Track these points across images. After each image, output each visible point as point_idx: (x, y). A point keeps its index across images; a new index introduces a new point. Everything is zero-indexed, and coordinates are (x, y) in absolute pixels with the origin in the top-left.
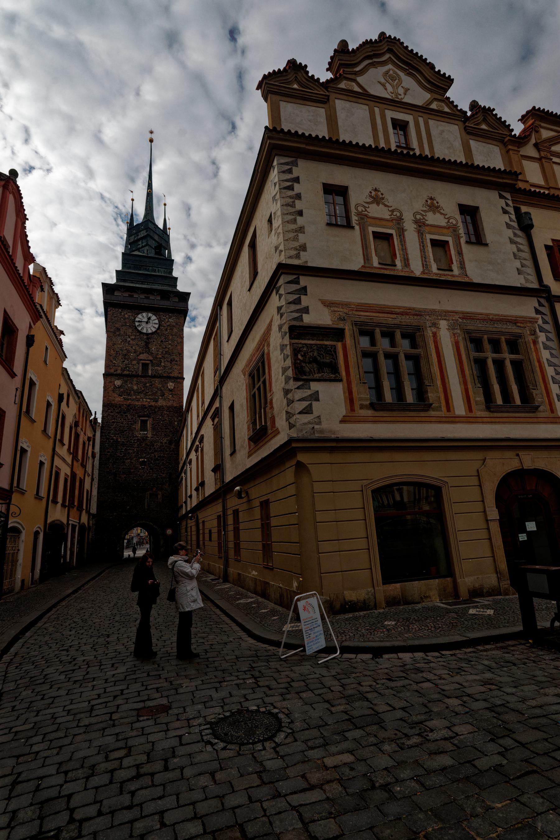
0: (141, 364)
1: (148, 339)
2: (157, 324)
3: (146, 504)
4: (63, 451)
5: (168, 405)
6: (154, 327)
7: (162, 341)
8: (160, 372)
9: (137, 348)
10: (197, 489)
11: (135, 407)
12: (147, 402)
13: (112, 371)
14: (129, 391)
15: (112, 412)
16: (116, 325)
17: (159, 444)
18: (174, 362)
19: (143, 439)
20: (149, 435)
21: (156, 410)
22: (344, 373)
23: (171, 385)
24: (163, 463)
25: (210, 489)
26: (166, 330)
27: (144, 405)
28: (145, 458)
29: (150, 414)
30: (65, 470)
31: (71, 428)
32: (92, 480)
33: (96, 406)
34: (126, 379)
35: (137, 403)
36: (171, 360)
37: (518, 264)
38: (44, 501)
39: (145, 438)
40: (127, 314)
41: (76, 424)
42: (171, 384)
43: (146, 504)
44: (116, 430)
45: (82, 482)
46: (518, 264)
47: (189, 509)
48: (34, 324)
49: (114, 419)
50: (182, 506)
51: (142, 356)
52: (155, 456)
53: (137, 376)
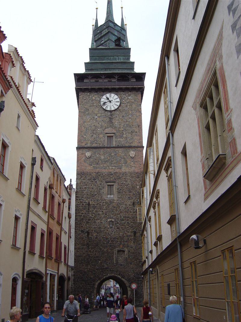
0: (106, 137)
1: (111, 115)
2: (118, 102)
3: (115, 259)
4: (39, 209)
5: (130, 171)
6: (116, 105)
7: (123, 116)
8: (123, 142)
9: (103, 124)
10: (156, 244)
11: (102, 174)
12: (112, 169)
13: (83, 145)
14: (97, 161)
15: (84, 180)
16: (86, 107)
17: (124, 206)
18: (134, 133)
19: (111, 202)
20: (116, 199)
21: (120, 176)
23: (132, 153)
24: (128, 223)
25: (166, 242)
26: (127, 106)
27: (110, 172)
28: (112, 218)
29: (115, 179)
30: (41, 226)
31: (45, 189)
32: (70, 237)
33: (70, 175)
34: (94, 150)
35: (104, 171)
36: (132, 132)
38: (22, 251)
39: (111, 202)
40: (94, 96)
41: (51, 187)
42: (132, 152)
43: (115, 259)
44: (88, 195)
45: (58, 238)
47: (150, 263)
48: (6, 93)
49: (86, 185)
50: (145, 261)
51: (107, 131)
52: (121, 217)
53: (104, 148)
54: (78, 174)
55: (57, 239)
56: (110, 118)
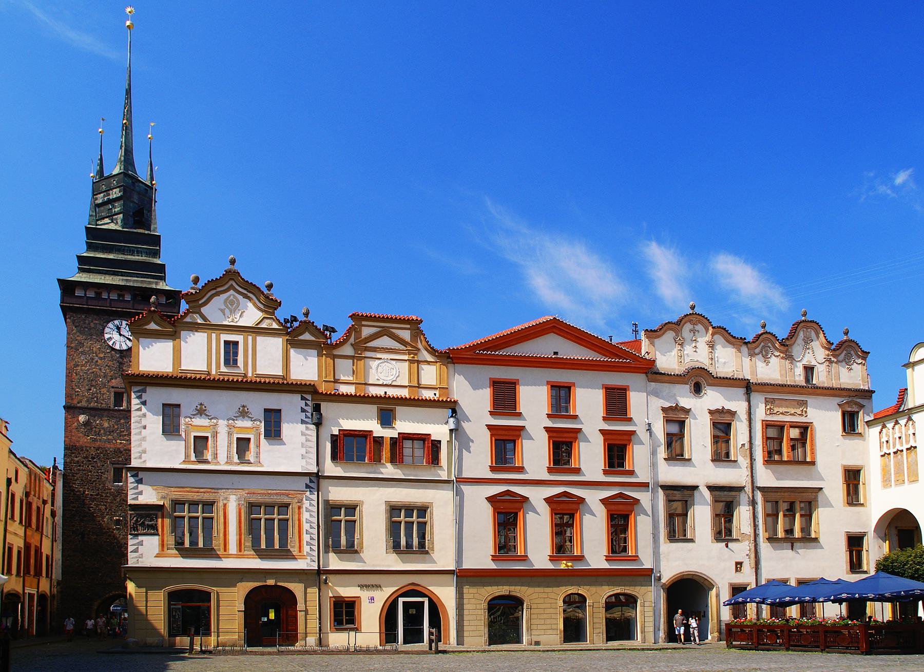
22: (160, 530)
37: (303, 451)
45: (38, 551)
46: (303, 451)
54: (66, 449)
55: (36, 551)
56: (121, 363)
